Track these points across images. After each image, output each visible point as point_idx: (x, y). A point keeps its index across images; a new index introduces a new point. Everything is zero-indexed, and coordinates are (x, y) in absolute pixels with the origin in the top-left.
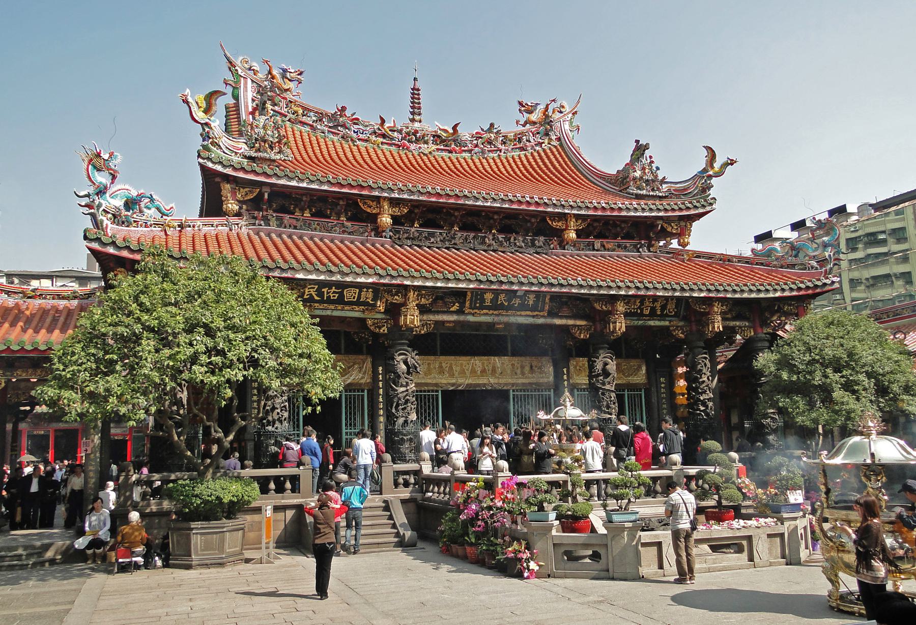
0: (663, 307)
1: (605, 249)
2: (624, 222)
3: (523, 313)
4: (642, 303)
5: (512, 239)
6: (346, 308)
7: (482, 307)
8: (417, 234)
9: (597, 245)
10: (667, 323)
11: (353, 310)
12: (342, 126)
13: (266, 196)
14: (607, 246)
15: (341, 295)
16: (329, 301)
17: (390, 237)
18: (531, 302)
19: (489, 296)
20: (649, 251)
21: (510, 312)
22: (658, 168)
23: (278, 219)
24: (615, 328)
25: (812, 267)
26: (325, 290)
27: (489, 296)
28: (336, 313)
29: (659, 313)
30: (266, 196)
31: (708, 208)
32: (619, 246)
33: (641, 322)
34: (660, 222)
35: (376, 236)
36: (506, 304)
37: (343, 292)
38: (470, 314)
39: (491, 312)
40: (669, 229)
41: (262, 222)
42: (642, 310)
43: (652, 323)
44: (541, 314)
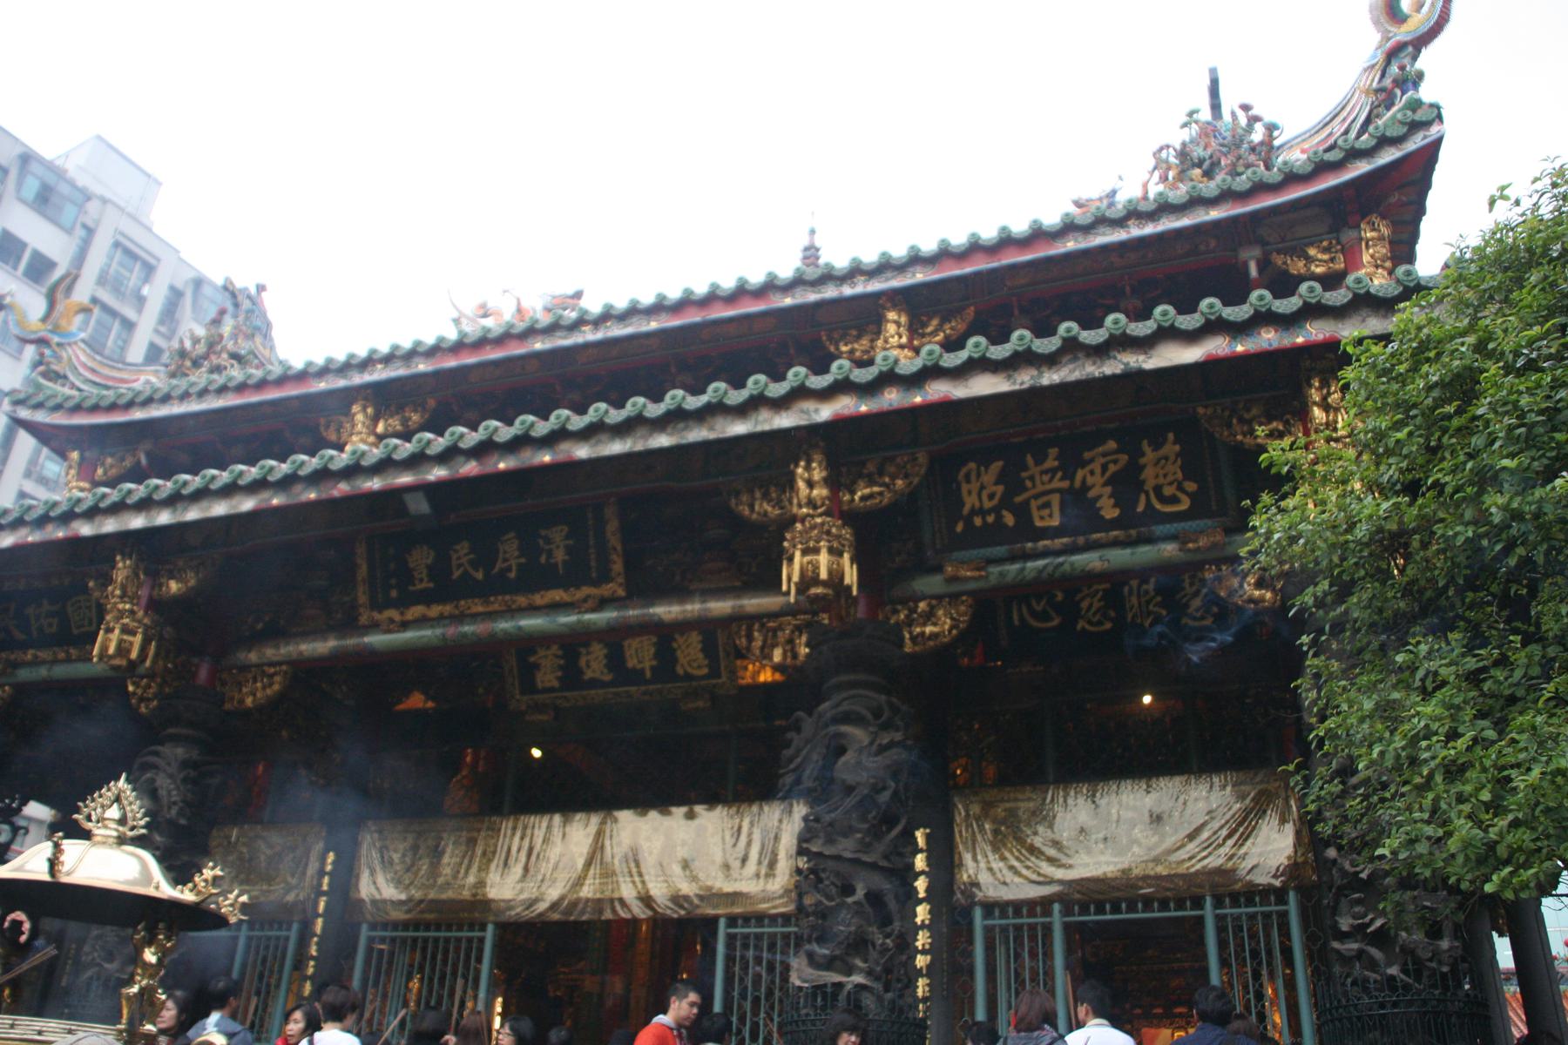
3: (538, 599)
6: (74, 652)
7: (403, 603)
10: (1169, 549)
18: (560, 556)
19: (420, 559)
22: (1271, 128)
26: (30, 611)
27: (420, 559)
29: (1110, 512)
31: (1415, 143)
34: (1256, 252)
36: (480, 576)
38: (375, 626)
39: (435, 611)
42: (1022, 512)
43: (1090, 560)
44: (607, 590)
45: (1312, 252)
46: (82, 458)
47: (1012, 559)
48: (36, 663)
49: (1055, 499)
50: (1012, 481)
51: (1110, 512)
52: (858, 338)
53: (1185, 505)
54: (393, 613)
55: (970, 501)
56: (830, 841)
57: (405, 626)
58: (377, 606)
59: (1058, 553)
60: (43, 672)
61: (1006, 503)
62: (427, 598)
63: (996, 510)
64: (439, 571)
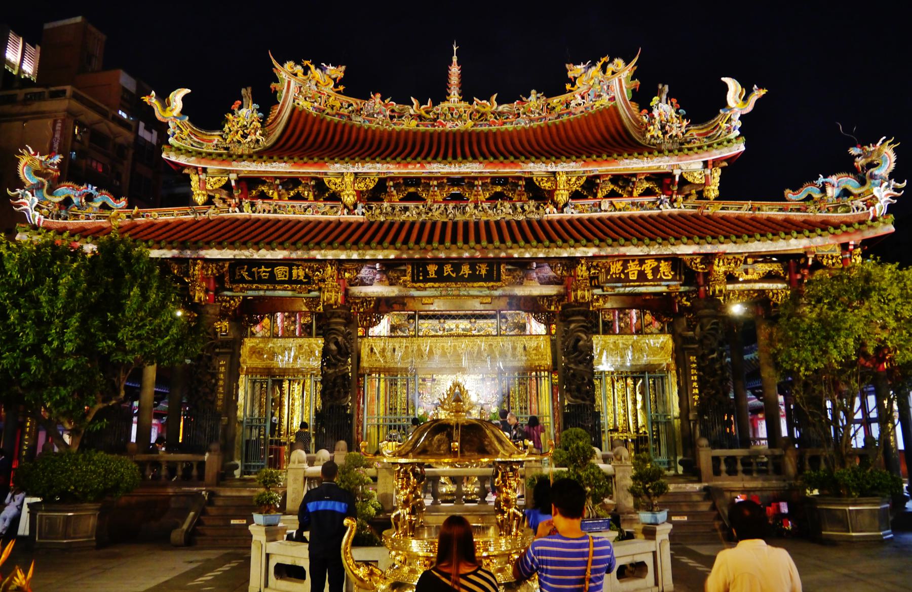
0: (655, 270)
1: (615, 210)
2: (635, 175)
3: (475, 284)
4: (625, 266)
5: (499, 206)
6: (278, 287)
7: (426, 280)
8: (389, 209)
9: (605, 204)
10: (664, 289)
11: (285, 289)
12: (378, 114)
13: (233, 183)
14: (618, 207)
15: (272, 274)
16: (261, 281)
17: (363, 214)
18: (483, 272)
19: (432, 269)
20: (674, 207)
21: (459, 285)
23: (253, 205)
24: (576, 296)
25: (858, 208)
27: (432, 269)
28: (269, 293)
29: (650, 277)
30: (233, 183)
32: (633, 204)
33: (628, 290)
35: (348, 214)
37: (273, 270)
39: (437, 285)
40: (690, 179)
41: (237, 209)
42: (627, 275)
44: (499, 284)
45: (695, 174)
46: (200, 179)
47: (622, 287)
48: (257, 289)
49: (636, 272)
50: (625, 266)
51: (650, 277)
52: (547, 182)
53: (670, 277)
54: (422, 285)
55: (612, 271)
56: (576, 365)
57: (425, 289)
58: (413, 281)
59: (634, 286)
60: (262, 293)
61: (623, 271)
62: (433, 280)
63: (620, 274)
64: (439, 272)
